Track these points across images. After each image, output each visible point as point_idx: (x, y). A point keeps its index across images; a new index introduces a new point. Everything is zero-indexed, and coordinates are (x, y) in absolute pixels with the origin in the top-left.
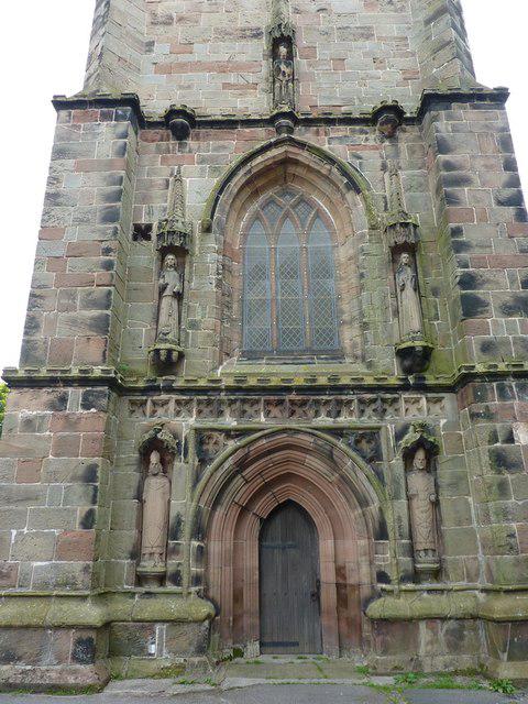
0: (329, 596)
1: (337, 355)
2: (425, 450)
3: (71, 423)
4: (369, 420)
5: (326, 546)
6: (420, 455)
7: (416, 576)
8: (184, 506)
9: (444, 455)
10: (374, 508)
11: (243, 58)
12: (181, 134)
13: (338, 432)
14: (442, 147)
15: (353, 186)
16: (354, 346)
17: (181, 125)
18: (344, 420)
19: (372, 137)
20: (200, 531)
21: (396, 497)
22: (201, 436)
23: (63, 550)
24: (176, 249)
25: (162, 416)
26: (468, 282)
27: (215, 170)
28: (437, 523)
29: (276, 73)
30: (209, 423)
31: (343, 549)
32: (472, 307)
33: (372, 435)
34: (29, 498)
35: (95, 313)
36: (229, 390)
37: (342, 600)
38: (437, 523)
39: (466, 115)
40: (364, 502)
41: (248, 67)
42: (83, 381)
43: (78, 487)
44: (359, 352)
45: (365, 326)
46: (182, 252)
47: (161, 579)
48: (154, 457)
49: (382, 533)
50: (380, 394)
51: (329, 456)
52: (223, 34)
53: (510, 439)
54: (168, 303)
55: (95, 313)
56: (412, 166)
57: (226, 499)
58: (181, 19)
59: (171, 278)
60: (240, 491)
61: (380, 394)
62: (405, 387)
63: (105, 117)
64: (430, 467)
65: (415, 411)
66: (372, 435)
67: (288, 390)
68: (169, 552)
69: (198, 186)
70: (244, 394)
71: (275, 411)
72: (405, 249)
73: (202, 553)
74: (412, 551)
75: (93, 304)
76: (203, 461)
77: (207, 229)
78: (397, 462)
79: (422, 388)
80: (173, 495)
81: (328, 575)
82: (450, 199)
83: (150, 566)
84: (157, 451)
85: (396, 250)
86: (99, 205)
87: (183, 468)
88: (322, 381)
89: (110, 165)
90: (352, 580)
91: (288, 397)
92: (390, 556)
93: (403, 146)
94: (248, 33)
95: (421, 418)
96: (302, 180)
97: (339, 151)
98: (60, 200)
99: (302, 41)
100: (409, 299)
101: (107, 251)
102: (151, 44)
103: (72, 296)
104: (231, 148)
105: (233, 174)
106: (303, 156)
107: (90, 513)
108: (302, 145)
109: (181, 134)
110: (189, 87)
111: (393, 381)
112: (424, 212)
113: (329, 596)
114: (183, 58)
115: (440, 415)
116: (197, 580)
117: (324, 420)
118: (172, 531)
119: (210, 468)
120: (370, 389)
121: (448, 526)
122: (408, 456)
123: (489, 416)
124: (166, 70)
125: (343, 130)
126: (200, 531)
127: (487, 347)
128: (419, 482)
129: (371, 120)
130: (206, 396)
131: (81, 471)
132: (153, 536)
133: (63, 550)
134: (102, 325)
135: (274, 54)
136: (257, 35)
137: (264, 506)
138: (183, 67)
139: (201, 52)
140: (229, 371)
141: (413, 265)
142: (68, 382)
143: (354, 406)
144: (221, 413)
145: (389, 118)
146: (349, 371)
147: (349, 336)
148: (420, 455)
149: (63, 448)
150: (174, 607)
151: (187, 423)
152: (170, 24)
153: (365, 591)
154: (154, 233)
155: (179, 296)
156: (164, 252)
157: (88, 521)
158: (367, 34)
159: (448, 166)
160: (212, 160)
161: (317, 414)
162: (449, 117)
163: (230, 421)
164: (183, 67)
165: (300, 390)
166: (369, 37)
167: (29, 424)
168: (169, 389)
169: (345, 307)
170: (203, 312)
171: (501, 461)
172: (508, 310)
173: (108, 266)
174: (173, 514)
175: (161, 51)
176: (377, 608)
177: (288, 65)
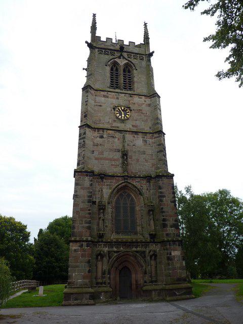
0: (134, 287)
1: (136, 233)
2: (154, 256)
3: (84, 251)
4: (143, 249)
5: (133, 276)
6: (153, 257)
7: (152, 282)
8: (106, 267)
9: (158, 257)
10: (144, 268)
11: (115, 157)
12: (102, 178)
13: (137, 252)
14: (160, 188)
15: (141, 194)
16: (140, 231)
17: (102, 176)
19: (144, 182)
20: (109, 273)
21: (148, 266)
22: (109, 252)
23: (84, 277)
24: (102, 208)
25: (99, 248)
26: (164, 220)
27: (110, 188)
28: (156, 270)
29: (123, 163)
30: (111, 250)
31: (137, 277)
32: (165, 226)
33: (144, 252)
34: (77, 267)
35: (87, 225)
36: (115, 242)
37: (137, 287)
38: (156, 270)
39: (165, 180)
40: (142, 267)
41: (117, 160)
42: (86, 241)
43: (87, 264)
44: (141, 233)
45: (143, 228)
46: (104, 209)
47: (101, 283)
48: (99, 257)
49: (145, 273)
50: (146, 244)
51: (135, 257)
52: (111, 150)
53: (171, 254)
54: (101, 222)
55: (87, 225)
57: (114, 266)
59: (102, 215)
61: (146, 244)
62: (151, 242)
63: (87, 176)
64: (155, 259)
65: (153, 247)
66: (144, 252)
67: (127, 242)
68: (103, 278)
69: (106, 192)
70: (118, 243)
71: (124, 247)
72: (151, 211)
73: (109, 278)
74: (151, 277)
75: (86, 223)
76: (110, 258)
77: (109, 203)
78: (149, 258)
79: (154, 242)
80: (103, 266)
81: (134, 282)
82: (161, 201)
83: (100, 281)
84: (100, 255)
85: (149, 211)
86: (87, 198)
88: (134, 240)
89: (88, 188)
90: (139, 283)
91: (127, 244)
92: (147, 278)
93: (151, 184)
95: (154, 249)
96: (129, 190)
99: (130, 154)
101: (89, 210)
102: (93, 151)
103: (82, 221)
104: (114, 183)
105: (114, 189)
106: (130, 186)
107: (90, 270)
108: (130, 183)
109: (102, 178)
111: (148, 241)
112: (155, 202)
113: (134, 287)
114: (101, 156)
115: (157, 248)
116: (109, 283)
117: (134, 249)
118: (103, 273)
119: (111, 259)
120: (144, 242)
121: (158, 272)
122: (151, 257)
123: (167, 249)
124: (96, 159)
125: (138, 180)
126: (109, 273)
127: (167, 235)
128: (153, 262)
129: (145, 177)
130: (110, 244)
131: (87, 261)
132: (100, 274)
133: (84, 277)
134: (89, 228)
135: (123, 157)
136: (119, 151)
137: (121, 267)
138: (101, 159)
139: (106, 155)
140: (114, 237)
141: (153, 214)
142: (83, 241)
143: (141, 246)
144: (113, 247)
145: (148, 178)
146: (139, 237)
147: (139, 229)
148: (153, 257)
149: (83, 256)
150: (105, 289)
151: (106, 249)
153: (142, 285)
154: (97, 203)
155: (103, 220)
156: (100, 209)
157: (89, 271)
158: (144, 153)
159: (161, 193)
160: (110, 185)
161: (133, 247)
163: (115, 249)
164: (101, 159)
165: (130, 242)
166: (145, 154)
167: (75, 250)
168: (102, 242)
169: (138, 221)
170: (109, 224)
171: (169, 259)
172: (171, 227)
173: (90, 214)
174: (104, 269)
175: (96, 153)
176: (145, 288)
177: (127, 161)
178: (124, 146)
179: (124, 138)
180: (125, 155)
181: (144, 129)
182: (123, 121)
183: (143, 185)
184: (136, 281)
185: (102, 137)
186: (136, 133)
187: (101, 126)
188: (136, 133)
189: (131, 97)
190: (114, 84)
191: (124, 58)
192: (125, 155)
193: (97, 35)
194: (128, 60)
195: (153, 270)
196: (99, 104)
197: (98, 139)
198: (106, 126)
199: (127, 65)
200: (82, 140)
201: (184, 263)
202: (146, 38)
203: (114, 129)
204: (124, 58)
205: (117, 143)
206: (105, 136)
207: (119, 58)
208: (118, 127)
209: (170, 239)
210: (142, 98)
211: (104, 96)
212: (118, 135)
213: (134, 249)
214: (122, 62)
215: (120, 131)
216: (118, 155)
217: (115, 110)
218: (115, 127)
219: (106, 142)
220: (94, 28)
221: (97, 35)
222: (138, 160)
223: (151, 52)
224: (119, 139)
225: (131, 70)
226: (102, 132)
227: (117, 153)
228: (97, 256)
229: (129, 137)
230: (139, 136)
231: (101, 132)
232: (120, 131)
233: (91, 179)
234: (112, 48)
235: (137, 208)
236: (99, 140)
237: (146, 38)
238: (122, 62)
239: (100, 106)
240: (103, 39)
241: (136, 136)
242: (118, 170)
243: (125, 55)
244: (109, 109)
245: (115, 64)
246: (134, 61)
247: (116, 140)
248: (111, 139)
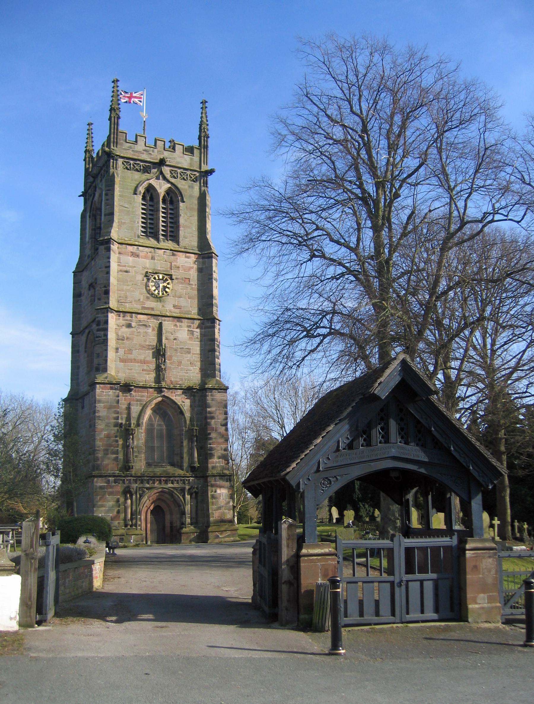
5: (168, 517)
18: (176, 485)
35: (114, 456)
42: (114, 476)
52: (142, 347)
53: (216, 492)
55: (114, 456)
58: (128, 338)
63: (111, 388)
81: (168, 524)
90: (175, 525)
94: (150, 347)
98: (101, 418)
99: (168, 354)
110: (131, 369)
117: (170, 485)
127: (213, 468)
142: (110, 476)
152: (123, 340)
153: (178, 527)
162: (212, 395)
166: (189, 353)
172: (219, 458)
175: (121, 351)
177: (164, 365)
180: (159, 353)
181: (189, 312)
182: (158, 298)
184: (171, 523)
185: (129, 326)
186: (179, 318)
187: (128, 307)
188: (179, 318)
189: (173, 255)
190: (151, 231)
192: (159, 353)
194: (172, 184)
197: (124, 329)
198: (136, 307)
199: (169, 192)
200: (101, 327)
202: (203, 136)
204: (165, 178)
206: (133, 324)
208: (152, 309)
210: (188, 257)
211: (133, 254)
212: (154, 323)
213: (170, 485)
214: (162, 187)
219: (136, 334)
222: (180, 363)
223: (209, 169)
224: (153, 330)
225: (174, 199)
226: (129, 318)
230: (182, 324)
231: (128, 317)
233: (117, 394)
237: (203, 136)
238: (162, 187)
239: (126, 272)
241: (178, 324)
243: (166, 170)
244: (140, 277)
245: (150, 189)
246: (182, 185)
247: (150, 330)
248: (142, 330)
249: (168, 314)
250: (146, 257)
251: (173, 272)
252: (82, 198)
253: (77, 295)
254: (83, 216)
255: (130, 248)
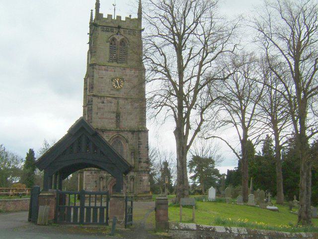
7: (130, 193)
19: (130, 134)
22: (107, 176)
26: (140, 159)
28: (133, 188)
32: (140, 162)
34: (89, 184)
38: (133, 187)
43: (95, 183)
52: (109, 112)
56: (135, 139)
60: (111, 183)
82: (139, 147)
85: (132, 153)
87: (105, 180)
97: (126, 136)
99: (121, 115)
100: (133, 160)
106: (121, 136)
118: (104, 188)
124: (99, 118)
125: (126, 132)
127: (141, 167)
128: (132, 182)
132: (102, 188)
135: (117, 117)
136: (114, 113)
141: (134, 155)
145: (133, 132)
149: (93, 178)
157: (96, 186)
164: (103, 118)
172: (144, 163)
175: (99, 114)
178: (117, 109)
179: (118, 103)
180: (118, 115)
183: (129, 136)
185: (103, 103)
187: (103, 94)
188: (127, 99)
189: (124, 69)
190: (114, 59)
191: (121, 35)
192: (118, 115)
193: (100, 12)
195: (132, 186)
196: (101, 77)
197: (101, 104)
201: (149, 183)
203: (112, 96)
205: (113, 107)
206: (105, 102)
207: (117, 34)
208: (114, 95)
209: (142, 170)
211: (105, 70)
212: (114, 101)
214: (119, 38)
215: (115, 98)
216: (114, 116)
217: (112, 80)
218: (112, 94)
220: (98, 5)
221: (100, 12)
226: (103, 99)
227: (113, 114)
228: (100, 178)
229: (121, 102)
232: (115, 98)
234: (111, 25)
235: (125, 151)
236: (101, 105)
240: (105, 16)
242: (112, 126)
244: (108, 80)
245: (114, 39)
246: (128, 36)
249: (121, 97)
250: (111, 71)
251: (124, 77)
252: (88, 45)
253: (85, 89)
254: (88, 53)
255: (104, 67)
